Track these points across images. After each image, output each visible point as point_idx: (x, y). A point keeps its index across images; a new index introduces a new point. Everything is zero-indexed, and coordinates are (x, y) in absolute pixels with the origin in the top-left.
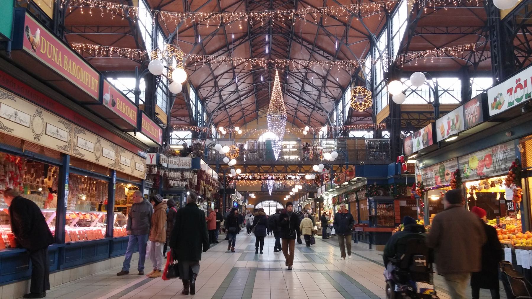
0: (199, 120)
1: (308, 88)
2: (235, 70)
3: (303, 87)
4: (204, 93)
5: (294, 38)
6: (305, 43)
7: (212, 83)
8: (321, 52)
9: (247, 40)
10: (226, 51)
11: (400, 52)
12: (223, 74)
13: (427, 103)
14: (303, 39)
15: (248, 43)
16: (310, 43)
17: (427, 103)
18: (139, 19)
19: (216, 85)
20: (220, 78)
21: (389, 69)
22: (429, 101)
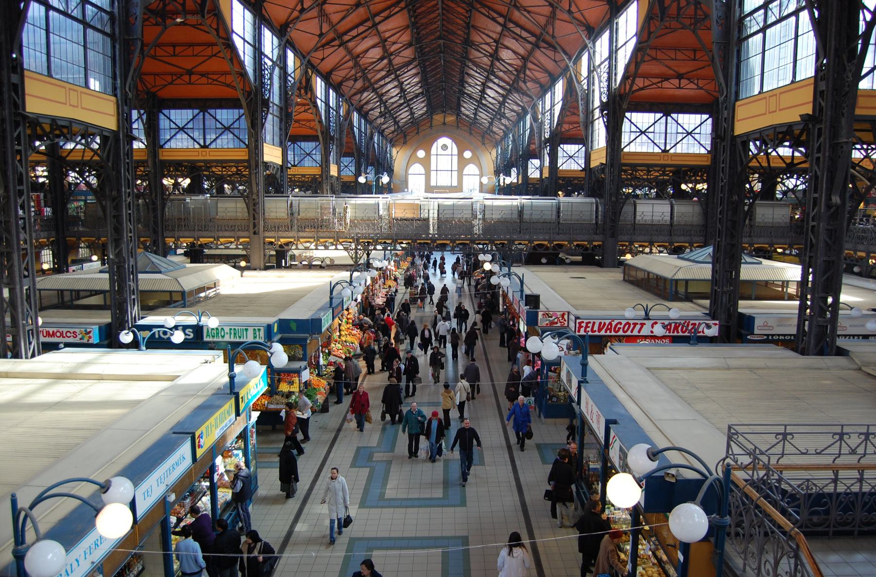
0: (331, 124)
2: (386, 43)
3: (492, 65)
7: (350, 64)
9: (402, 9)
10: (370, 28)
11: (625, 77)
12: (367, 51)
13: (660, 151)
14: (490, 8)
15: (405, 11)
16: (501, 15)
17: (660, 151)
18: (233, 31)
19: (357, 64)
22: (663, 148)
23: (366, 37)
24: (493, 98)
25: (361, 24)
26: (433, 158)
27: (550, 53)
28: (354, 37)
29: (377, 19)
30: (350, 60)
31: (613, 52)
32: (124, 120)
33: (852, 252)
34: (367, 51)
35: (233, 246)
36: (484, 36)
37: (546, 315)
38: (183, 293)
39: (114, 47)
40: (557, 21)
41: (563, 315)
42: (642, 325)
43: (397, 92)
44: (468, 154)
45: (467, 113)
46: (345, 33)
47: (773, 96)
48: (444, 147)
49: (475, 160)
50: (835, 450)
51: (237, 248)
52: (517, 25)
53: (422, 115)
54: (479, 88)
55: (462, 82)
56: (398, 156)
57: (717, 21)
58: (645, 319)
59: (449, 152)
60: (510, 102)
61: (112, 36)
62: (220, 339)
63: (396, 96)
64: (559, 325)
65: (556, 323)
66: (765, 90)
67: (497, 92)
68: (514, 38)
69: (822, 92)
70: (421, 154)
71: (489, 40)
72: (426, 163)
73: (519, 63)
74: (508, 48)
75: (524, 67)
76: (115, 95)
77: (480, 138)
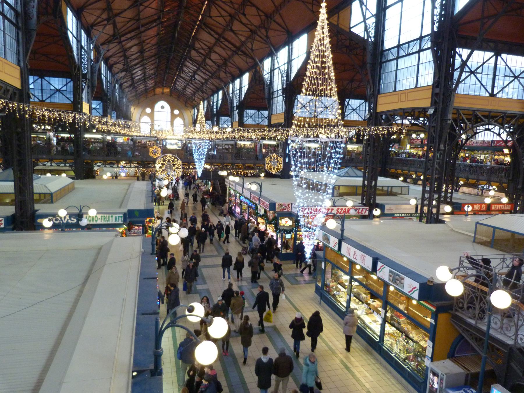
1: (208, 61)
3: (204, 60)
4: (112, 61)
5: (203, 27)
6: (213, 33)
8: (226, 43)
12: (131, 47)
16: (217, 33)
20: (129, 51)
21: (286, 84)
23: (134, 39)
24: (198, 80)
25: (133, 31)
26: (156, 113)
27: (245, 58)
28: (128, 39)
29: (143, 29)
30: (122, 51)
31: (290, 62)
32: (24, 82)
33: (407, 172)
34: (131, 47)
35: (49, 164)
36: (202, 45)
37: (280, 205)
38: (51, 194)
39: (18, 34)
40: (255, 41)
41: (288, 205)
42: (332, 209)
43: (141, 73)
44: (176, 112)
45: (179, 87)
46: (123, 35)
47: (403, 93)
48: (162, 107)
49: (181, 115)
50: (501, 266)
51: (65, 166)
52: (226, 40)
53: (152, 87)
54: (190, 74)
55: (181, 70)
56: (134, 111)
57: (370, 53)
58: (333, 207)
59: (165, 110)
60: (209, 83)
61: (16, 25)
62: (95, 223)
63: (140, 75)
64: (286, 210)
65: (285, 209)
66: (397, 90)
67: (202, 77)
68: (222, 47)
69: (437, 94)
70: (148, 110)
71: (205, 47)
72: (151, 116)
73: (220, 61)
74: (216, 52)
75: (225, 64)
76: (19, 65)
77: (184, 103)
